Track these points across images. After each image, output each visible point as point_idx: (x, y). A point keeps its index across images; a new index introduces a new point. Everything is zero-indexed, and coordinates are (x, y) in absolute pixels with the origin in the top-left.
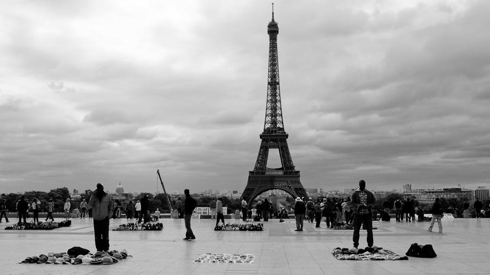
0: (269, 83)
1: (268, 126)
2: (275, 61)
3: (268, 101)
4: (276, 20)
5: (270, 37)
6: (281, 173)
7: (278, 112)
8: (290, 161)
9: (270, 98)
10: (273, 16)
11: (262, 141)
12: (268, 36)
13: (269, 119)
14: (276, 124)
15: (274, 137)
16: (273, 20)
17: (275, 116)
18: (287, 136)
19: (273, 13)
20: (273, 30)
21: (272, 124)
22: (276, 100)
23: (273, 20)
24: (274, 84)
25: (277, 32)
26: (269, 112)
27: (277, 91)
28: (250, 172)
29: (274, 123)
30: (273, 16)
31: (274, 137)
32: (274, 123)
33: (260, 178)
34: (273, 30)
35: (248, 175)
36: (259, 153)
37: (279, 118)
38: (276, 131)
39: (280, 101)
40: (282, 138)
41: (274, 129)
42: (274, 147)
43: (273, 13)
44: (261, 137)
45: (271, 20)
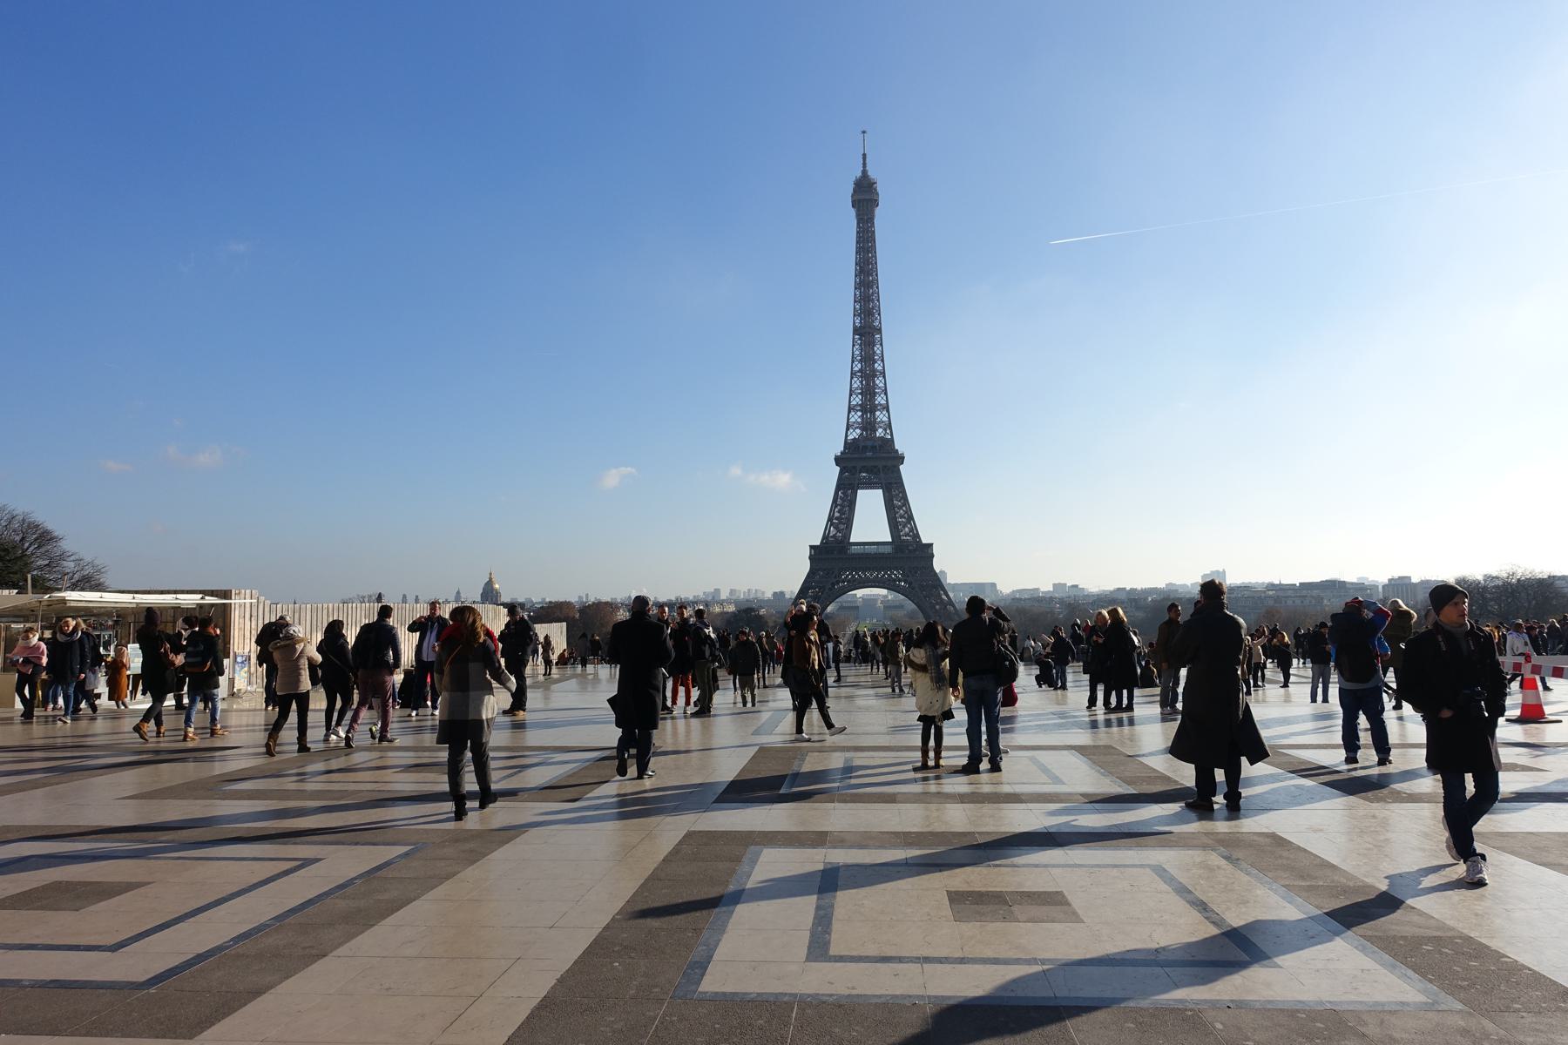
0: (856, 331)
1: (854, 434)
2: (870, 274)
3: (853, 374)
4: (872, 174)
5: (858, 215)
6: (888, 549)
7: (880, 400)
8: (911, 518)
9: (858, 367)
10: (864, 164)
11: (841, 473)
12: (853, 212)
13: (856, 417)
14: (875, 431)
15: (870, 461)
16: (864, 172)
17: (873, 411)
18: (901, 459)
19: (864, 156)
20: (865, 196)
21: (863, 429)
22: (874, 370)
23: (864, 172)
24: (867, 333)
25: (875, 203)
26: (857, 400)
27: (877, 349)
28: (812, 547)
29: (869, 426)
30: (864, 164)
31: (870, 461)
32: (869, 426)
33: (835, 560)
34: (865, 196)
35: (807, 553)
36: (835, 501)
37: (881, 416)
38: (873, 447)
39: (883, 373)
40: (889, 463)
41: (869, 443)
42: (870, 485)
43: (864, 156)
44: (838, 460)
45: (859, 174)
